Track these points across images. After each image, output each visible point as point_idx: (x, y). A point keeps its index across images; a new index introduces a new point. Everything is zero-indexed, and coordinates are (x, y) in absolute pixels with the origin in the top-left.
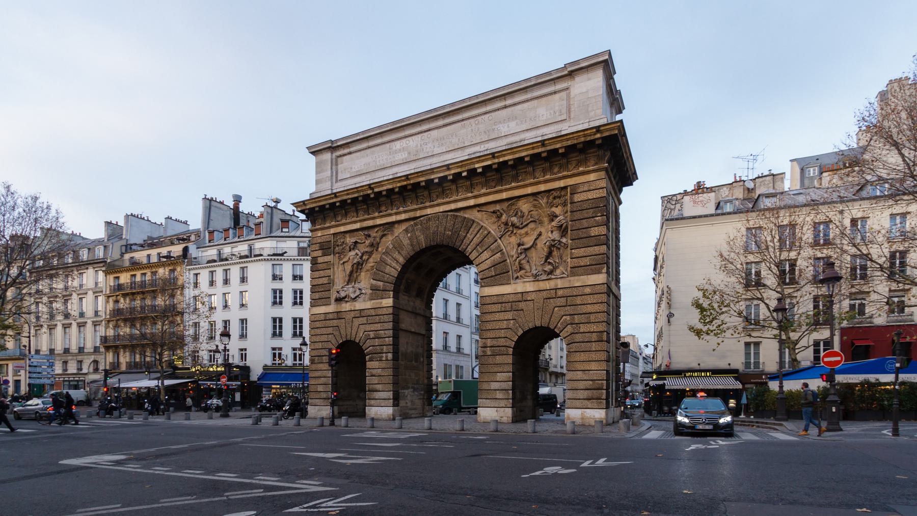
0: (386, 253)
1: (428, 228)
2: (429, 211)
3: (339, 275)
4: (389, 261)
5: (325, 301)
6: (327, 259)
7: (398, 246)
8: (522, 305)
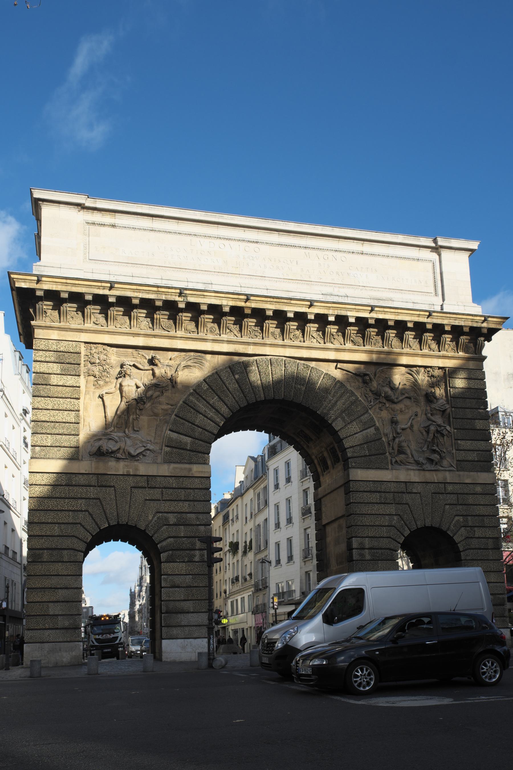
4: (201, 406)
8: (407, 498)
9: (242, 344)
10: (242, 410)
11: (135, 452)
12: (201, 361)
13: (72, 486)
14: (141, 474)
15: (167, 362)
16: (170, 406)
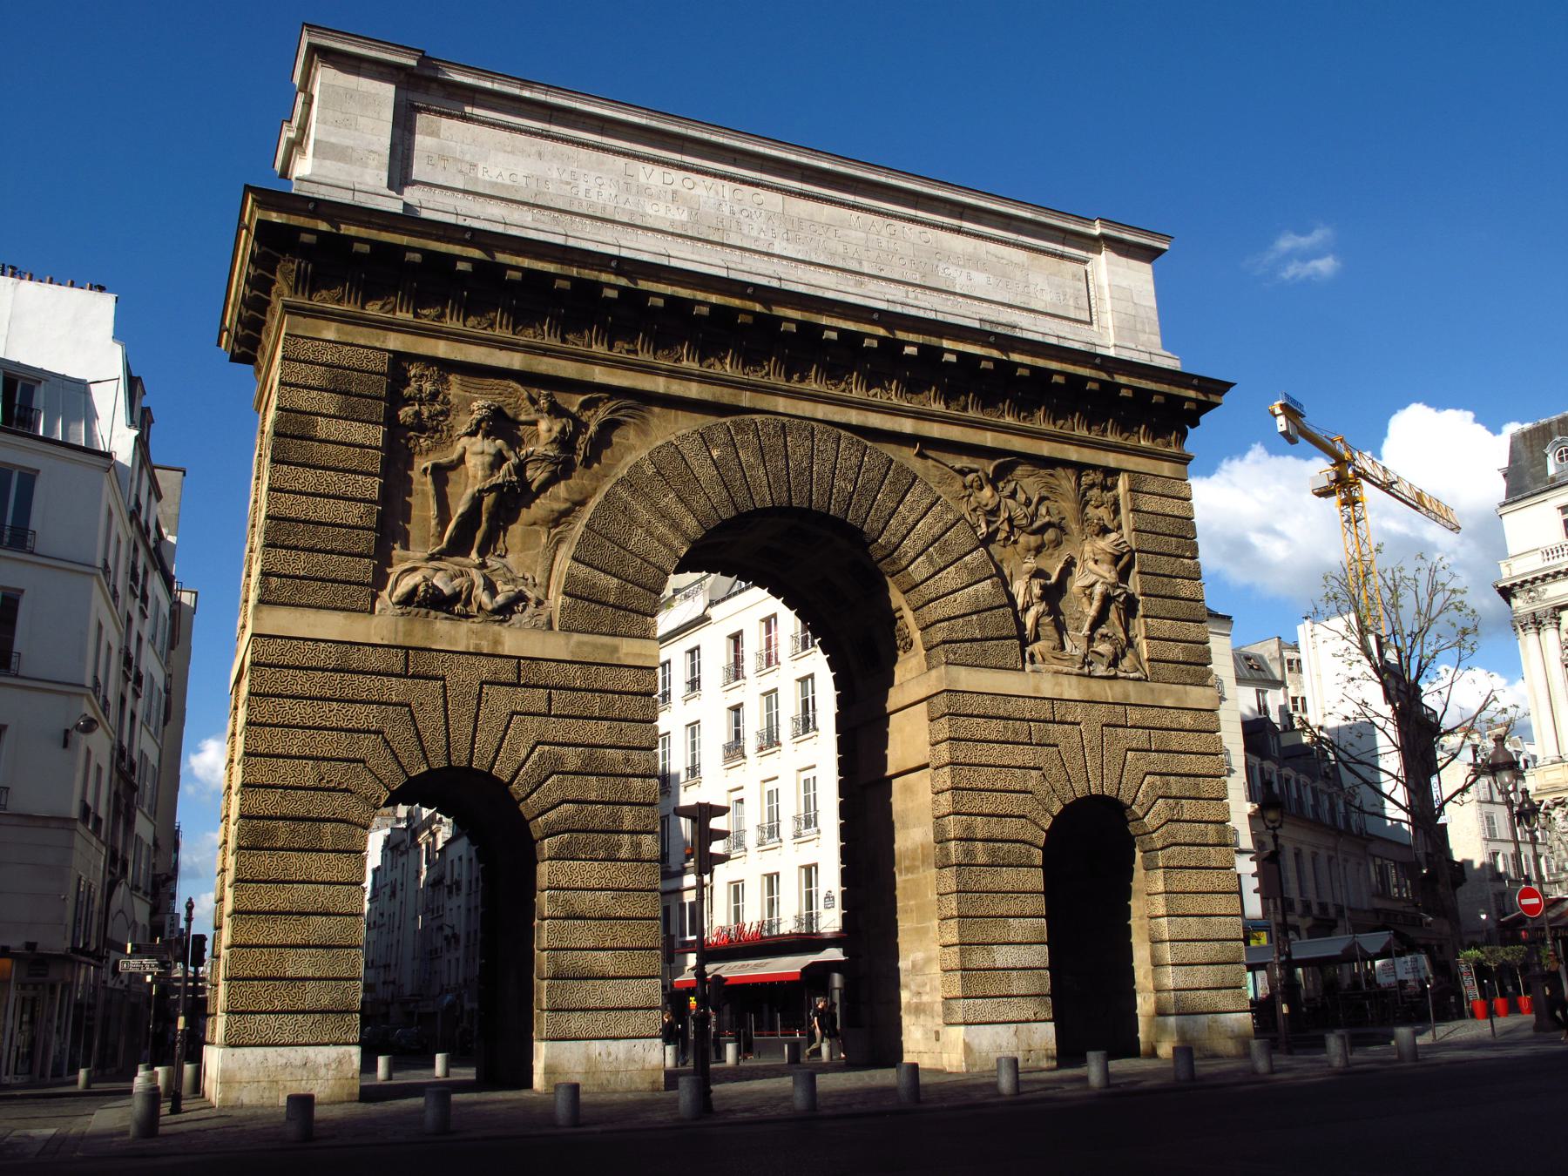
2: (782, 404)
10: (725, 526)
13: (348, 671)
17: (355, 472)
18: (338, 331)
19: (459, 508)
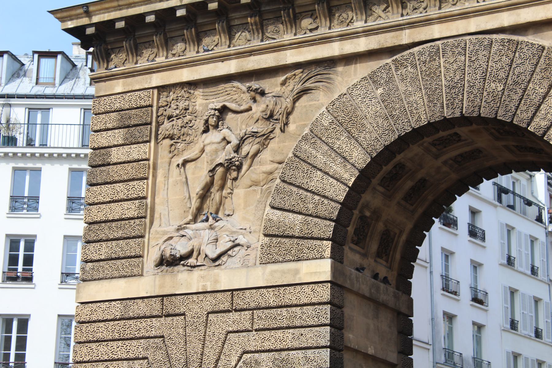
0: (314, 136)
1: (433, 75)
2: (437, 31)
3: (172, 194)
4: (320, 157)
5: (127, 263)
6: (136, 151)
7: (345, 119)
9: (389, 31)
11: (214, 252)
12: (327, 76)
14: (222, 289)
15: (278, 89)
16: (276, 165)
17: (133, 180)
18: (124, 85)
19: (197, 188)
